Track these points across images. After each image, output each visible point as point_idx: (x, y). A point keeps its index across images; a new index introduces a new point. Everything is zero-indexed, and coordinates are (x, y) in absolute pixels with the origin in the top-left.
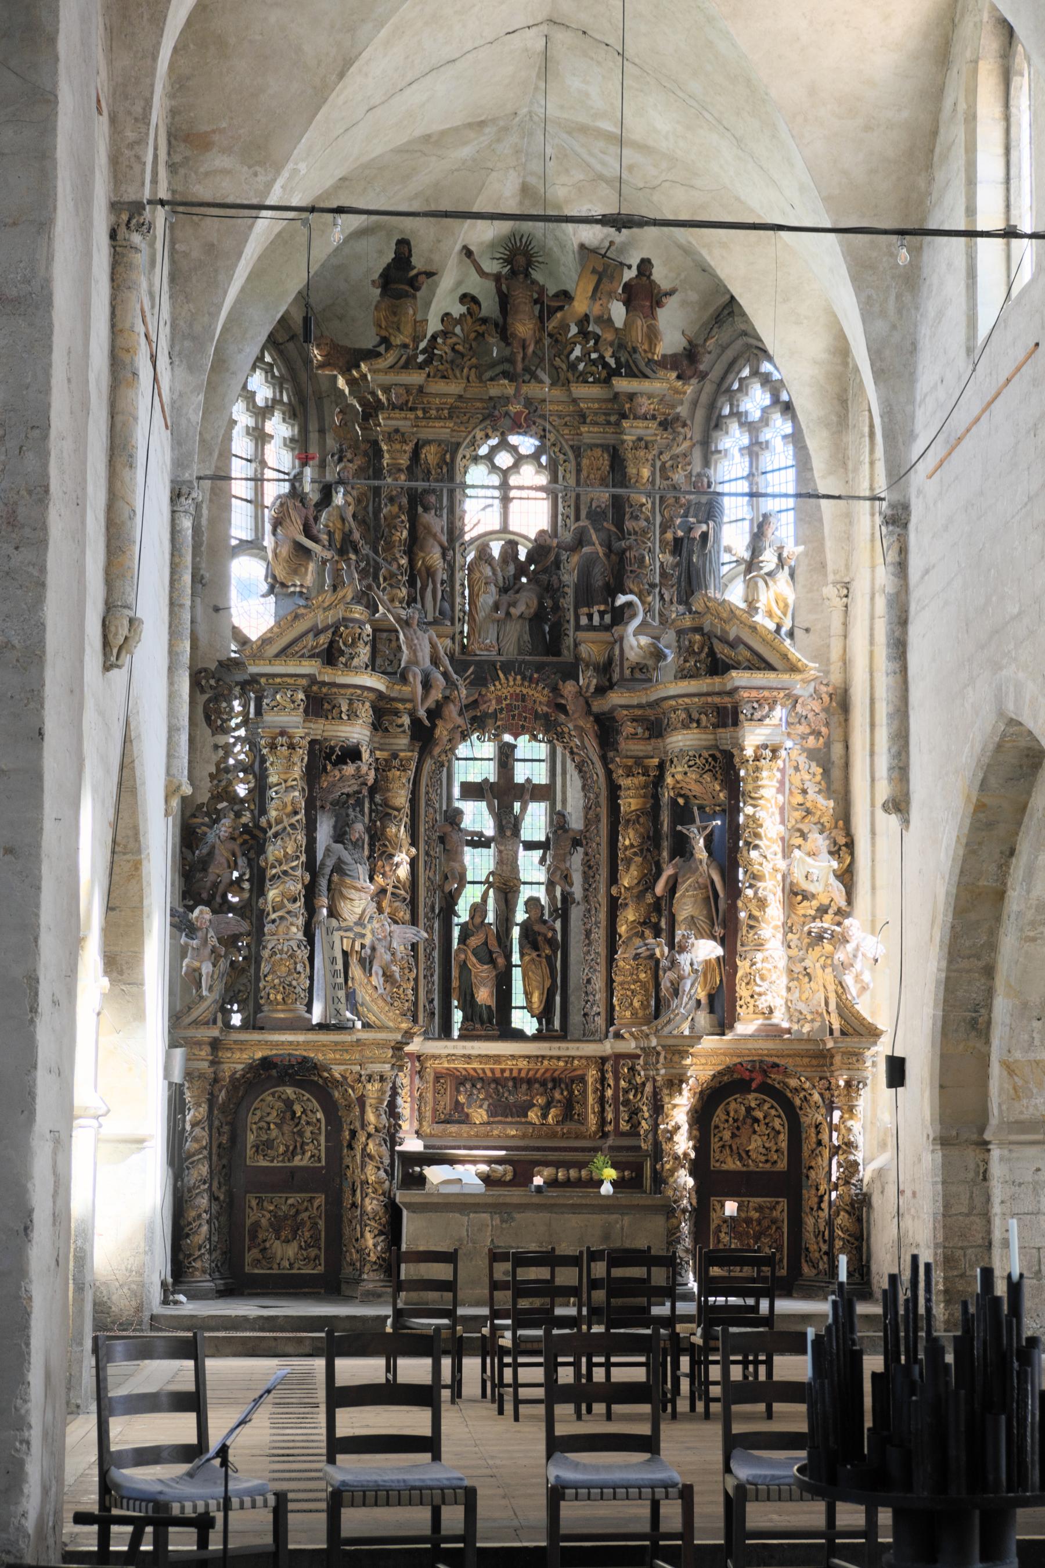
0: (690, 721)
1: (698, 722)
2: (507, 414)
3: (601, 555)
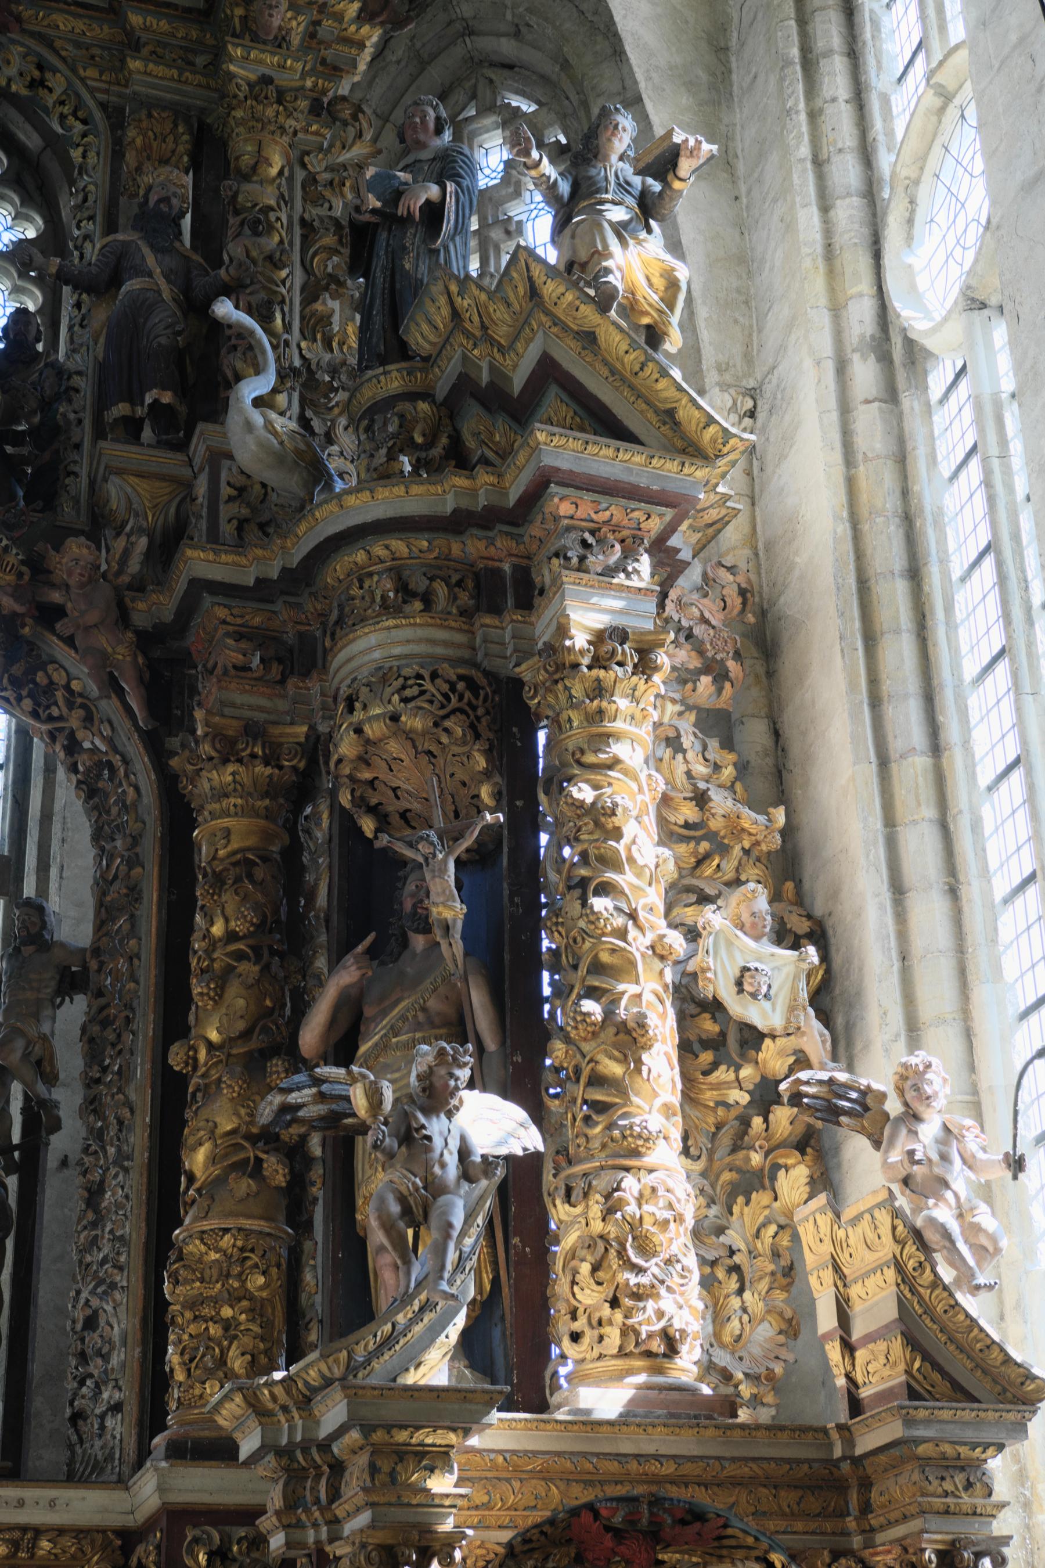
0: (407, 594)
1: (427, 600)
3: (166, 295)
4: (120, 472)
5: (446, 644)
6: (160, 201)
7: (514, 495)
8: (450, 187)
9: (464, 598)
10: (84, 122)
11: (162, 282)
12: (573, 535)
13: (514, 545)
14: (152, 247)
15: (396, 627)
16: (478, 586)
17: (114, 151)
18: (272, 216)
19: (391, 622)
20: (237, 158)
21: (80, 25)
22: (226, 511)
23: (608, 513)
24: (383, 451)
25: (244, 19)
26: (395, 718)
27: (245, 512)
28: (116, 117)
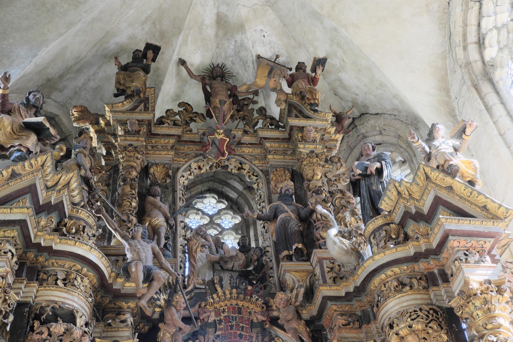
2: (213, 142)
4: (289, 271)
5: (421, 299)
6: (286, 191)
7: (434, 245)
8: (383, 162)
9: (423, 283)
10: (256, 176)
11: (291, 213)
12: (461, 252)
13: (437, 262)
14: (286, 204)
15: (402, 296)
16: (427, 279)
17: (267, 182)
18: (322, 189)
19: (400, 295)
20: (307, 176)
21: (251, 150)
22: (328, 276)
23: (471, 243)
24: (383, 241)
25: (302, 137)
26: (410, 327)
27: (334, 275)
28: (266, 173)
